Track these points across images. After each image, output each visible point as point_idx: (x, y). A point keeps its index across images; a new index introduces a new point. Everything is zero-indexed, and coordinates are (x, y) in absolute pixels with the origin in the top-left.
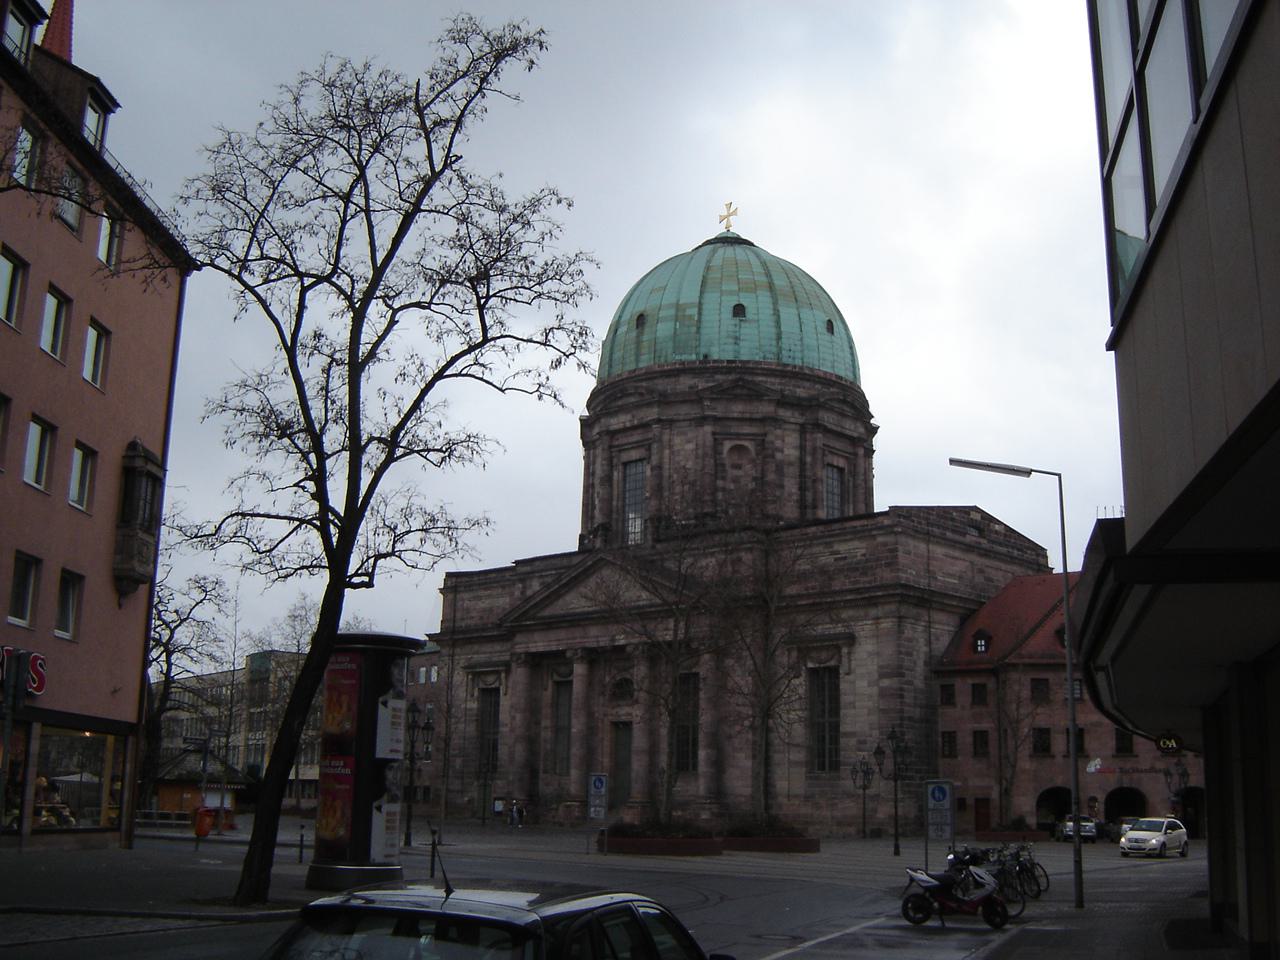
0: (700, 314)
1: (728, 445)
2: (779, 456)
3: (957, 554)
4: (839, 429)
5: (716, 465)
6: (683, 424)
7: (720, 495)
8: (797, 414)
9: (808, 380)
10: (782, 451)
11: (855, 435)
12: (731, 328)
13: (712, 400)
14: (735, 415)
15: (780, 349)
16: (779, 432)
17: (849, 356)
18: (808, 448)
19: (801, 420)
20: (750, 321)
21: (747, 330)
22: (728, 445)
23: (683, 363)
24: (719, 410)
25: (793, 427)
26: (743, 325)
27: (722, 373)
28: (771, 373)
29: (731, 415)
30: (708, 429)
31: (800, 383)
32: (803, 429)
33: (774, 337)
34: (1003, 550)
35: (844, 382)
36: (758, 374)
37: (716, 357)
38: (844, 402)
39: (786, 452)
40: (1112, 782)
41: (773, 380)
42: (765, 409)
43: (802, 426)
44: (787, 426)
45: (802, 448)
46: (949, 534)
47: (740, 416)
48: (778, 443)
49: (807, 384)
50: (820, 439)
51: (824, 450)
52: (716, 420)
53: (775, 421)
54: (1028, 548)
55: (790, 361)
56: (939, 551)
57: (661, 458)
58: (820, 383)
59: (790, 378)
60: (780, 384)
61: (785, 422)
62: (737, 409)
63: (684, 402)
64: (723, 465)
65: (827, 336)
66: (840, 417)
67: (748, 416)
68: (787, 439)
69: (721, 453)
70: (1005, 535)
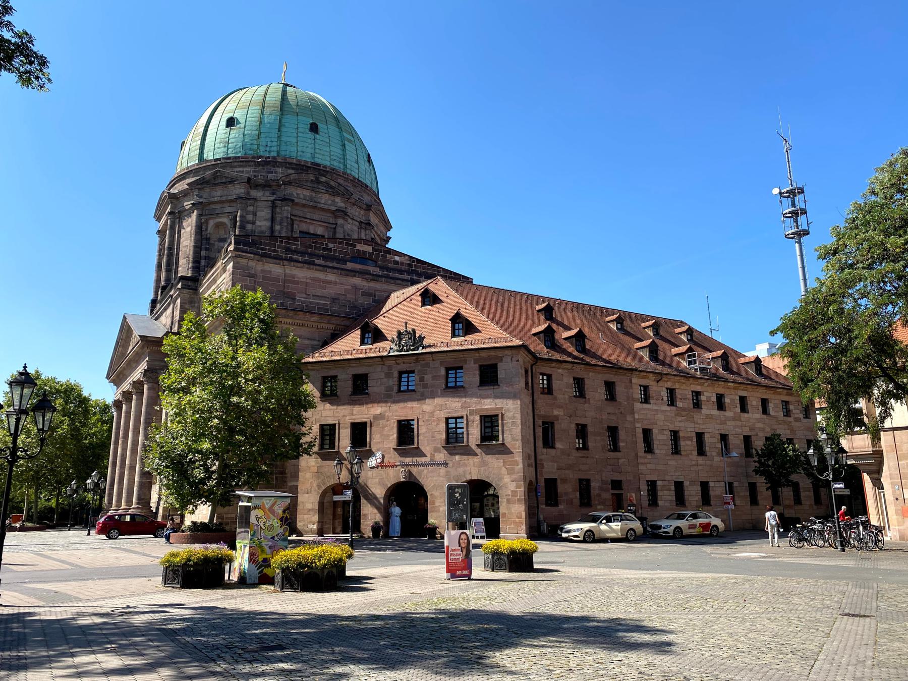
1: (211, 223)
2: (249, 227)
4: (311, 204)
8: (267, 193)
10: (254, 223)
11: (333, 208)
17: (340, 152)
18: (278, 219)
23: (188, 168)
34: (406, 277)
37: (211, 158)
38: (317, 181)
39: (258, 223)
40: (396, 475)
42: (238, 190)
43: (273, 202)
44: (260, 204)
45: (273, 220)
48: (250, 217)
55: (267, 154)
58: (293, 169)
62: (218, 193)
64: (208, 239)
65: (311, 135)
67: (224, 198)
68: (259, 214)
70: (410, 265)
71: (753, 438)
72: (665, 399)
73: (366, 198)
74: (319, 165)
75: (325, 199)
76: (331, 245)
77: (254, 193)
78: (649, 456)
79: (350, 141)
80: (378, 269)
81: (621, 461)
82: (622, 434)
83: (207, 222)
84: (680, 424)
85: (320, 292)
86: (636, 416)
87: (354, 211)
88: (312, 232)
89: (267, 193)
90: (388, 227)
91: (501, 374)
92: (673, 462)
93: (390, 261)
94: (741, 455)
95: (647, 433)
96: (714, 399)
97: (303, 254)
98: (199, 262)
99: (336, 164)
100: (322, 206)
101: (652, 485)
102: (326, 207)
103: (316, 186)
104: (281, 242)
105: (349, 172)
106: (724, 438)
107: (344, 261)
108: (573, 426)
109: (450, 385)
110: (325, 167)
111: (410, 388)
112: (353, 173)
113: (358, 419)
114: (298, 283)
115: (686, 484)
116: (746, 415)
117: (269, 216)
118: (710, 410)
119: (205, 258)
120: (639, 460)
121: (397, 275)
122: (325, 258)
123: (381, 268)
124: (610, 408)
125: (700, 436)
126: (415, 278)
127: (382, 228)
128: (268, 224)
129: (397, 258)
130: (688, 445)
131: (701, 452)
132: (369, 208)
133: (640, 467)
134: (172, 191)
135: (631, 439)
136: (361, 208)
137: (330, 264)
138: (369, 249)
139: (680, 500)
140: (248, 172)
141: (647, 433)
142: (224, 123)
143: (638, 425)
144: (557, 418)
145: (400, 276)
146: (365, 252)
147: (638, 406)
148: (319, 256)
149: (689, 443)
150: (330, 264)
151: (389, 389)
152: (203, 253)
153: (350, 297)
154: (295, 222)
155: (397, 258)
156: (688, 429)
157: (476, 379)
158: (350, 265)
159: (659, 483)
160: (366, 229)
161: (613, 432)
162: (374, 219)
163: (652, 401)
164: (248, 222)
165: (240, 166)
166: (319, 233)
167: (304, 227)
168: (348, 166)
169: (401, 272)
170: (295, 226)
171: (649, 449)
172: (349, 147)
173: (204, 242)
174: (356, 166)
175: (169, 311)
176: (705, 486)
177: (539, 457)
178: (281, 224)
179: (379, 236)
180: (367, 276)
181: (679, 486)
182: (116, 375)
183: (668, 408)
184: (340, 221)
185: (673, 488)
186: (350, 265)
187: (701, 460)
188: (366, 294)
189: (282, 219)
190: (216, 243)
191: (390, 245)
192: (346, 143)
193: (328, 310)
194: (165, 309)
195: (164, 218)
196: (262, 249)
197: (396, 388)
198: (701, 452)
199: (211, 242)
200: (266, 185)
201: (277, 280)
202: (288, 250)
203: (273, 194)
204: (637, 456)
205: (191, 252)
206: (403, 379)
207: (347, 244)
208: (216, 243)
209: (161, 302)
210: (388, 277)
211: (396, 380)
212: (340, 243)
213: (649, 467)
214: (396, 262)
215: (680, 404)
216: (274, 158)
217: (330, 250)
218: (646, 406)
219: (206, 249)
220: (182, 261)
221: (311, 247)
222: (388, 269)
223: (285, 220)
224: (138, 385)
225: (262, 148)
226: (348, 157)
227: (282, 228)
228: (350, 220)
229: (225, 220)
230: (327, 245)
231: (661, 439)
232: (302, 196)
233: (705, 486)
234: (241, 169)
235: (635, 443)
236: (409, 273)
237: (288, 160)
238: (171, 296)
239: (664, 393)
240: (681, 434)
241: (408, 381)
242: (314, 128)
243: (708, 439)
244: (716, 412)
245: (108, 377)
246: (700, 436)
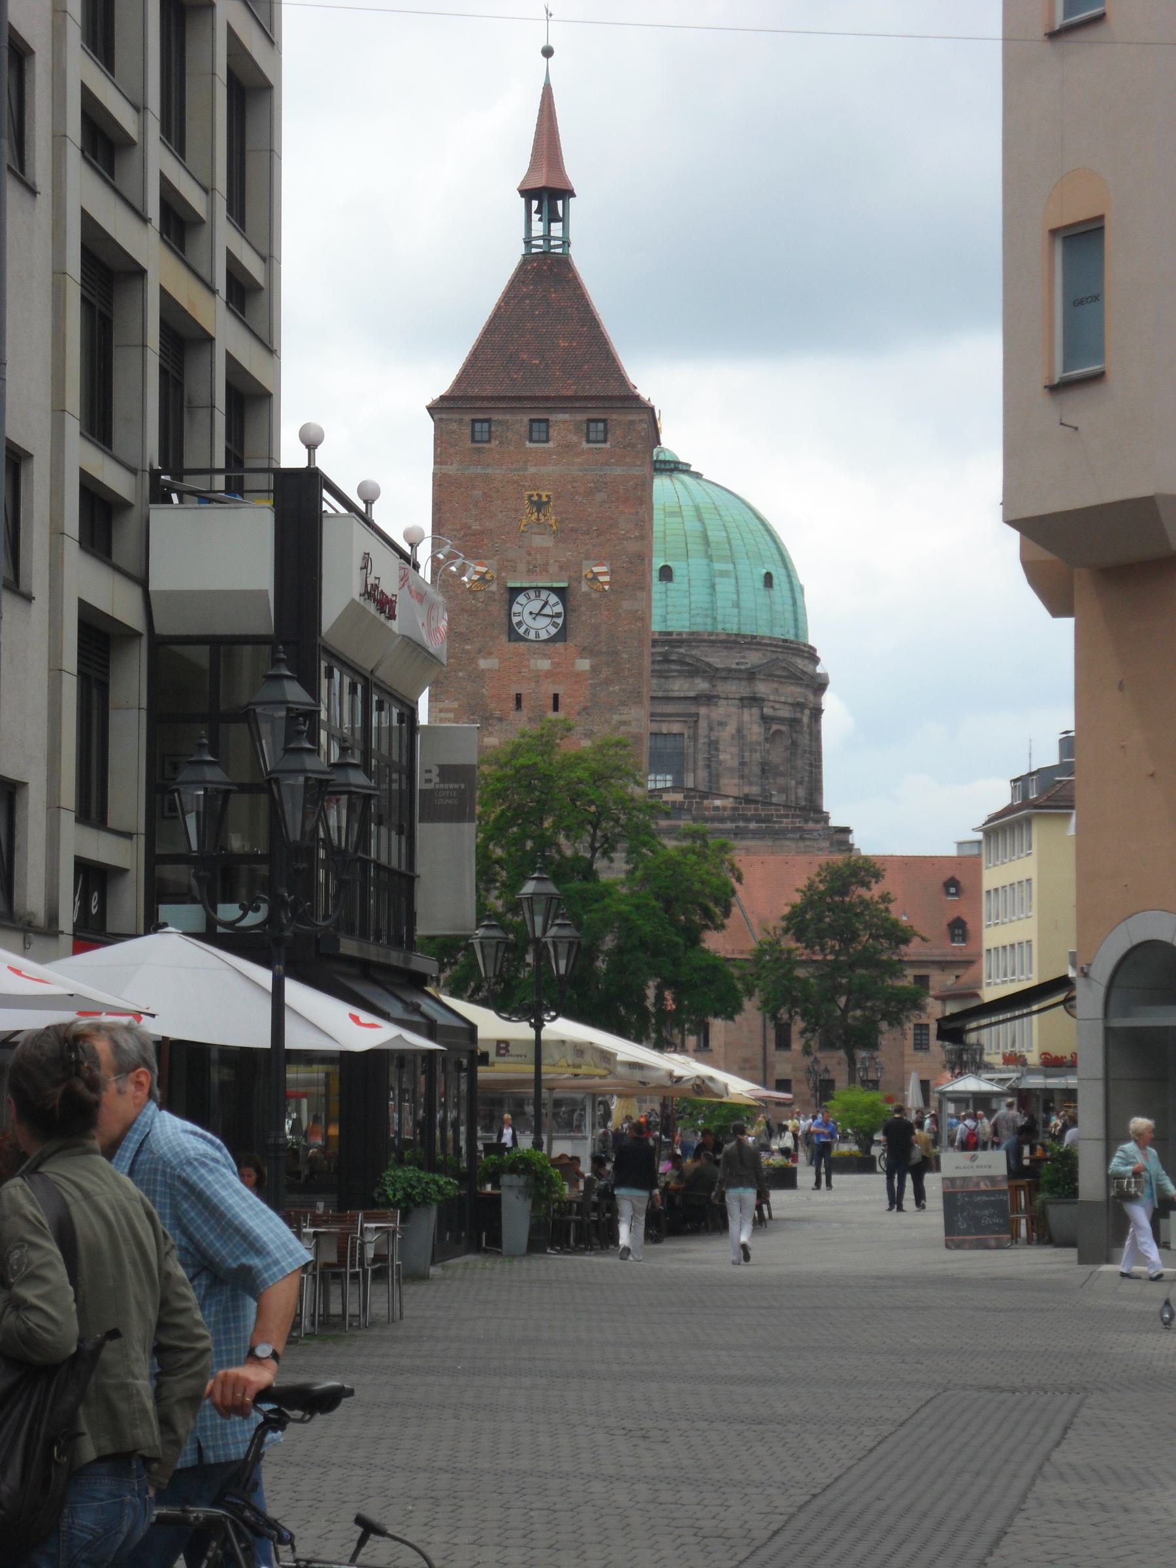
11: (692, 694)
34: (729, 825)
35: (674, 637)
66: (663, 680)
70: (734, 809)
74: (670, 634)
88: (665, 731)
93: (707, 809)
99: (699, 620)
100: (676, 694)
102: (682, 694)
103: (666, 667)
110: (679, 634)
112: (728, 626)
123: (695, 820)
126: (741, 824)
146: (674, 803)
160: (751, 707)
168: (719, 618)
169: (722, 820)
174: (735, 611)
177: (770, 1059)
184: (703, 711)
214: (717, 808)
222: (707, 820)
226: (719, 603)
236: (733, 820)
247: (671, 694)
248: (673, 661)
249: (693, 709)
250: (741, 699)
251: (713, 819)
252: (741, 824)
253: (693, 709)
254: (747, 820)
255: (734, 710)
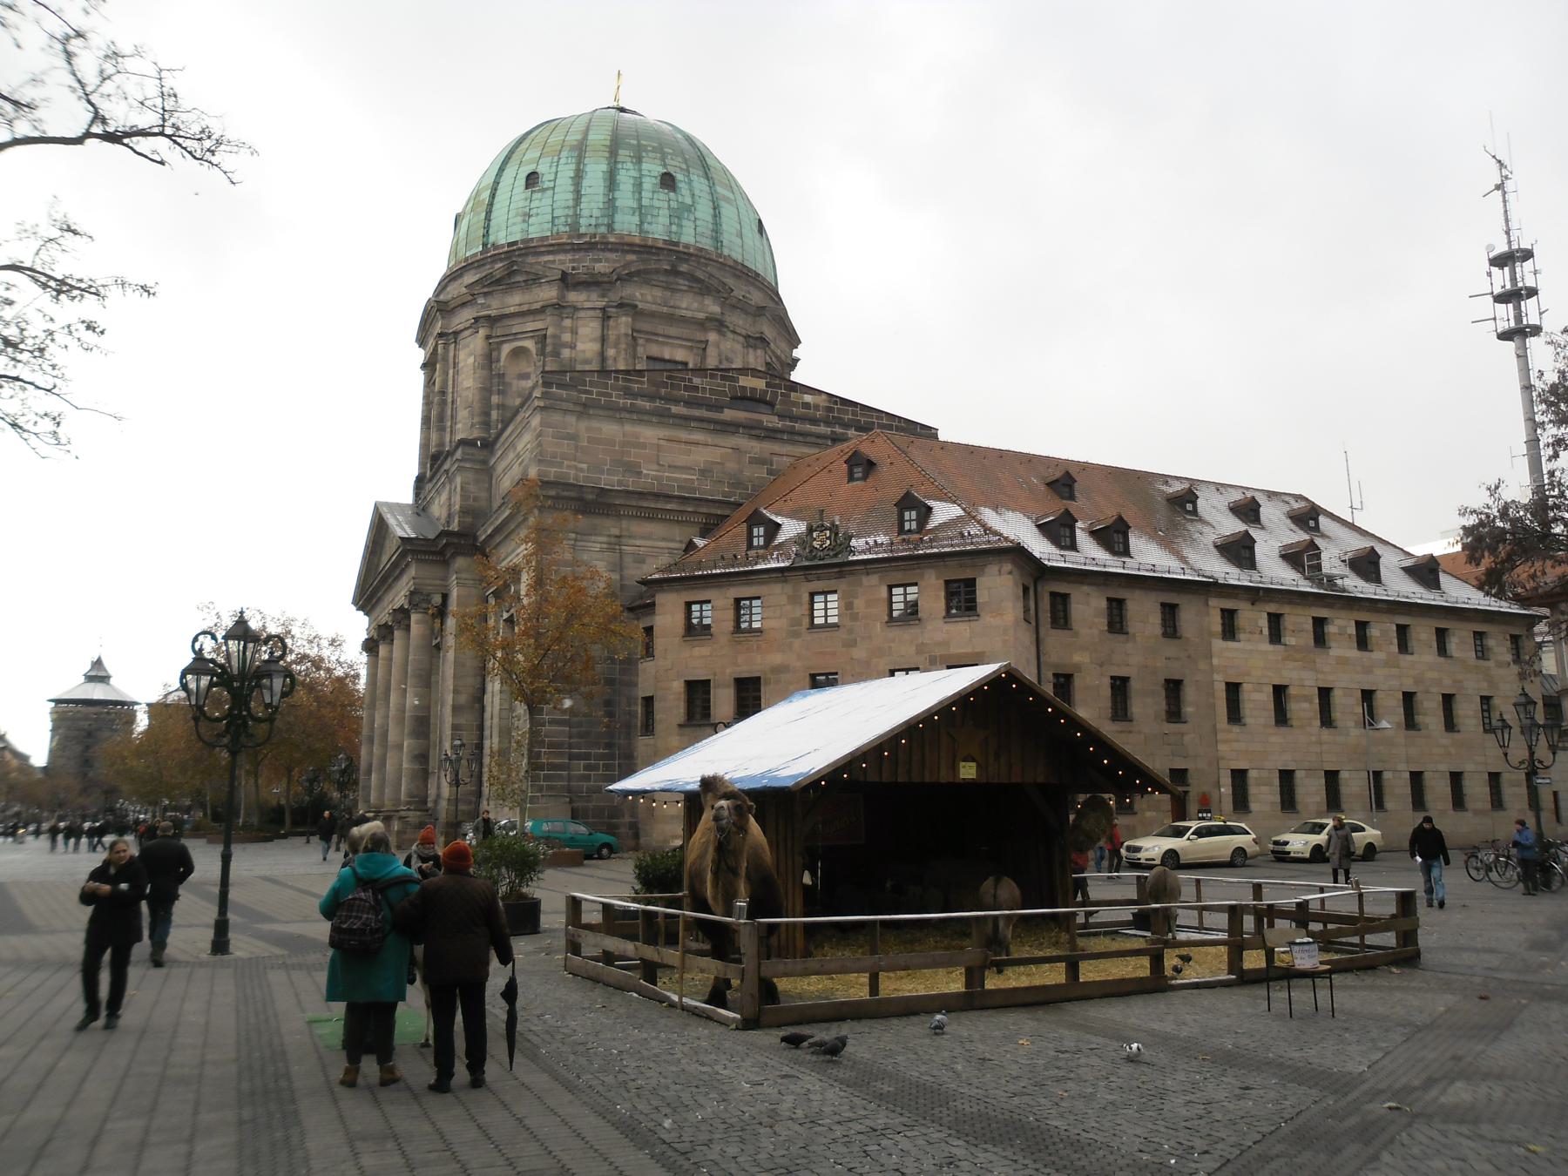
0: (493, 196)
1: (506, 349)
2: (566, 353)
3: (698, 436)
5: (491, 377)
6: (467, 333)
7: (494, 415)
9: (617, 251)
10: (573, 347)
11: (701, 316)
12: (521, 204)
13: (485, 294)
14: (512, 310)
15: (577, 216)
16: (567, 323)
19: (601, 304)
20: (544, 190)
21: (541, 203)
22: (506, 349)
24: (495, 305)
25: (592, 313)
26: (536, 196)
27: (501, 260)
28: (559, 248)
29: (507, 311)
30: (482, 332)
31: (602, 255)
32: (605, 317)
33: (571, 203)
34: (823, 429)
36: (542, 253)
37: (503, 242)
38: (674, 272)
39: (580, 346)
41: (561, 257)
42: (548, 293)
43: (603, 309)
44: (582, 314)
45: (603, 340)
46: (674, 409)
47: (517, 309)
48: (567, 337)
49: (613, 256)
50: (623, 323)
51: (634, 339)
52: (492, 321)
53: (559, 308)
54: (890, 427)
55: (592, 230)
56: (650, 434)
57: (445, 382)
58: (634, 252)
59: (586, 250)
60: (573, 261)
61: (576, 309)
62: (514, 301)
63: (464, 304)
64: (501, 376)
67: (525, 308)
68: (582, 331)
69: (498, 361)
71: (1419, 697)
72: (1266, 631)
73: (756, 298)
75: (688, 304)
76: (697, 381)
77: (574, 297)
78: (1236, 729)
79: (727, 200)
80: (776, 419)
81: (1187, 739)
82: (1190, 693)
83: (499, 350)
84: (1290, 674)
85: (682, 460)
86: (1215, 661)
87: (737, 320)
88: (667, 357)
89: (594, 296)
90: (794, 341)
91: (982, 596)
92: (1278, 737)
93: (795, 404)
94: (1398, 724)
95: (1233, 689)
96: (1352, 630)
97: (652, 398)
98: (487, 414)
99: (704, 240)
100: (683, 313)
101: (1239, 776)
102: (689, 314)
103: (671, 279)
104: (617, 379)
105: (726, 252)
106: (1367, 696)
107: (718, 408)
108: (1107, 681)
109: (817, 621)
110: (687, 246)
111: (830, 620)
113: (745, 671)
114: (644, 446)
115: (1299, 775)
116: (1408, 657)
117: (598, 333)
118: (1342, 647)
119: (499, 407)
120: (1219, 737)
121: (809, 427)
122: (689, 403)
123: (781, 417)
124: (1171, 648)
125: (1325, 693)
126: (838, 430)
127: (783, 345)
128: (596, 347)
129: (808, 398)
130: (1303, 709)
131: (1327, 719)
132: (760, 311)
133: (1221, 747)
134: (442, 297)
135: (1204, 701)
136: (747, 313)
137: (697, 413)
138: (760, 384)
139: (1288, 800)
140: (562, 262)
141: (1233, 689)
142: (522, 182)
143: (1216, 677)
144: (1078, 667)
145: (813, 429)
146: (753, 390)
147: (1219, 644)
148: (676, 401)
149: (1305, 705)
150: (697, 413)
151: (796, 622)
152: (495, 399)
153: (731, 466)
154: (641, 341)
155: (808, 398)
156: (1303, 682)
157: (941, 604)
158: (728, 414)
159: (1252, 774)
160: (755, 348)
161: (1174, 688)
162: (769, 332)
163: (1242, 636)
164: (565, 345)
165: (549, 253)
166: (678, 358)
167: (655, 350)
169: (814, 421)
170: (640, 350)
171: (1235, 715)
172: (727, 211)
173: (495, 380)
175: (444, 496)
176: (1332, 777)
178: (616, 345)
179: (778, 358)
180: (757, 432)
181: (1287, 777)
182: (366, 598)
183: (1271, 648)
185: (1277, 782)
186: (728, 414)
187: (1326, 734)
188: (758, 461)
189: (618, 337)
190: (515, 382)
191: (796, 376)
192: (722, 203)
193: (694, 490)
194: (438, 492)
195: (431, 342)
196: (586, 392)
197: (806, 621)
198: (1327, 719)
199: (507, 379)
200: (592, 283)
201: (611, 442)
202: (628, 393)
203: (604, 296)
204: (1215, 731)
205: (477, 398)
206: (816, 606)
207: (723, 378)
208: (515, 382)
209: (431, 480)
210: (792, 432)
211: (806, 606)
212: (712, 376)
213: (1235, 748)
214: (806, 405)
215: (1289, 639)
216: (603, 236)
217: (696, 388)
218: (1231, 644)
219: (499, 392)
220: (463, 414)
221: (665, 385)
222: (793, 418)
223: (623, 339)
224: (402, 615)
225: (583, 221)
227: (618, 353)
228: (730, 335)
229: (530, 344)
230: (690, 380)
231: (1257, 702)
232: (649, 298)
233: (1332, 777)
234: (551, 258)
235: (1213, 707)
236: (828, 423)
237: (627, 239)
238: (447, 471)
239: (1264, 623)
240: (1292, 691)
241: (826, 609)
242: (668, 181)
243: (1337, 698)
244: (1353, 653)
245: (355, 602)
246: (1325, 693)
247: (678, 312)
248: (681, 273)
249: (700, 336)
250: (747, 337)
251: (803, 419)
252: (838, 430)
253: (700, 336)
254: (846, 426)
255: (738, 347)
